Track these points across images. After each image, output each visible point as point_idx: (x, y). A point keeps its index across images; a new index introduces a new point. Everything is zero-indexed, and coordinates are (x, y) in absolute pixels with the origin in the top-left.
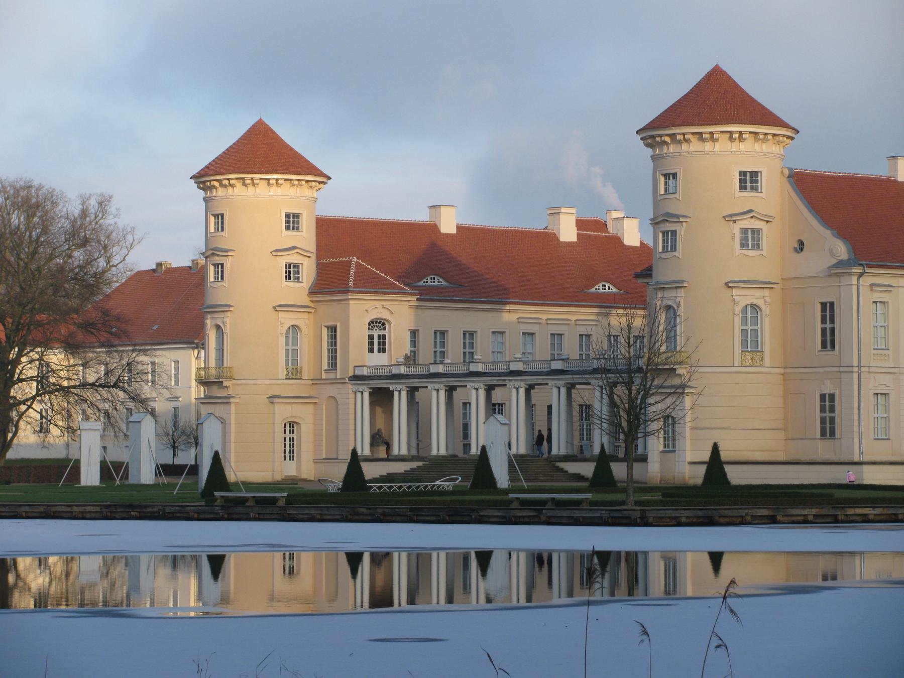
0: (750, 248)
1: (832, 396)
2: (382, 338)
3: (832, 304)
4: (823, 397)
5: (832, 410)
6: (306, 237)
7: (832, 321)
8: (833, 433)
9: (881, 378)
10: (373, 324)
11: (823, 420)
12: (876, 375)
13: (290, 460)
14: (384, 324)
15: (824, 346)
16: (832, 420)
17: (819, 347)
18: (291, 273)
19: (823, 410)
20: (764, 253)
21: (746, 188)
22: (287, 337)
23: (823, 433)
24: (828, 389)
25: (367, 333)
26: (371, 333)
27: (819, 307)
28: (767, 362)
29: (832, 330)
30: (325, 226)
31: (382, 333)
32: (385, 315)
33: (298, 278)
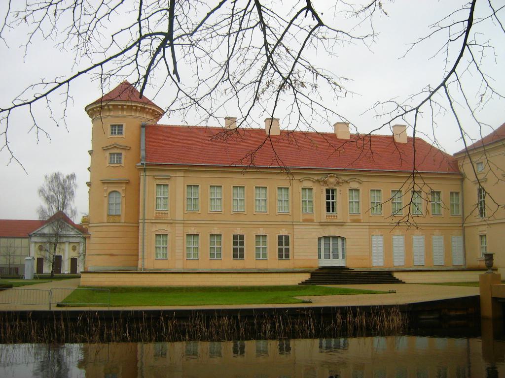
21: (115, 133)
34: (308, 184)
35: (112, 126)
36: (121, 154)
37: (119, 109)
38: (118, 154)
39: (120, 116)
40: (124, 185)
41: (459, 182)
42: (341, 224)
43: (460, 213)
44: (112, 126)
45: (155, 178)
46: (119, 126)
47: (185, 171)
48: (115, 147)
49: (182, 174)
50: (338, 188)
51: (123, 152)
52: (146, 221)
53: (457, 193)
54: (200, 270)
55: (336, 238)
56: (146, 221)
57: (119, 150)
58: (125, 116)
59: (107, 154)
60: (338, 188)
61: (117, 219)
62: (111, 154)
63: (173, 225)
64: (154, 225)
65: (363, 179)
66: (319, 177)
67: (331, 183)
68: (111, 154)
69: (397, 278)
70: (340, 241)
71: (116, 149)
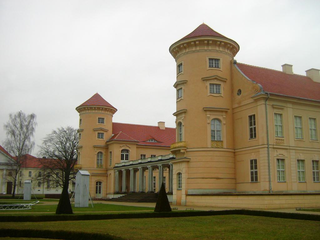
0: (215, 93)
1: (256, 161)
3: (254, 115)
4: (252, 161)
5: (256, 168)
8: (256, 179)
10: (122, 151)
11: (252, 173)
12: (278, 150)
13: (99, 193)
14: (127, 151)
15: (251, 136)
16: (256, 172)
20: (222, 95)
23: (252, 180)
25: (121, 153)
26: (122, 153)
27: (248, 119)
28: (225, 146)
31: (127, 154)
32: (127, 148)
33: (103, 138)
35: (210, 59)
36: (219, 85)
37: (192, 46)
38: (216, 85)
39: (217, 51)
40: (224, 114)
44: (210, 59)
45: (273, 107)
46: (215, 60)
47: (293, 103)
48: (216, 79)
49: (290, 105)
51: (222, 84)
52: (270, 146)
54: (309, 192)
56: (267, 146)
57: (219, 81)
58: (221, 52)
59: (208, 84)
61: (219, 144)
62: (210, 84)
63: (288, 150)
64: (275, 150)
68: (210, 84)
71: (216, 80)
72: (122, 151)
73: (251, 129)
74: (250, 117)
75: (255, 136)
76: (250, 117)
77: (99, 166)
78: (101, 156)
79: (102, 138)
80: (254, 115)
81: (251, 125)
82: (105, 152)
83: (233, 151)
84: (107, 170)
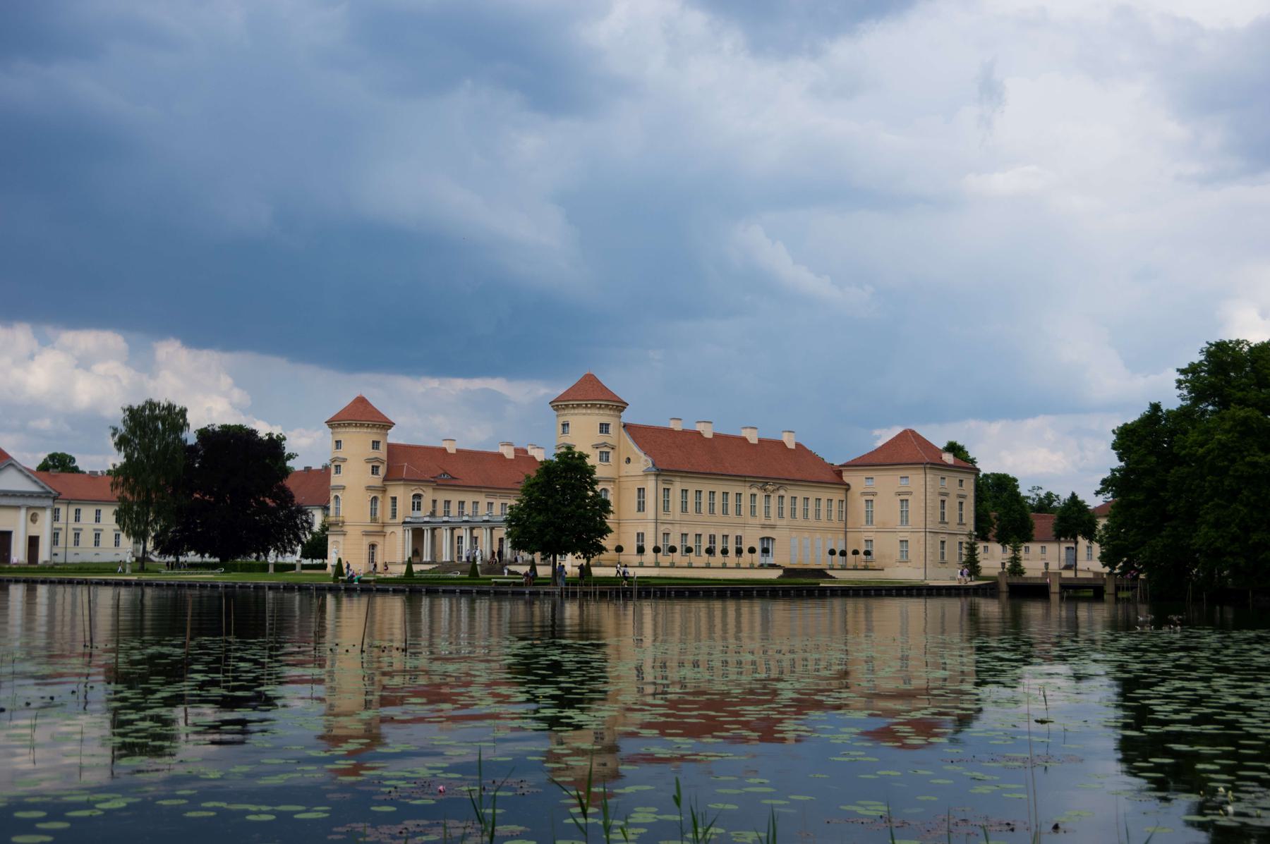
1: (643, 534)
2: (419, 504)
3: (644, 489)
4: (638, 534)
5: (643, 541)
6: (382, 453)
7: (644, 497)
9: (666, 526)
15: (639, 510)
17: (636, 509)
18: (375, 470)
19: (638, 541)
22: (372, 503)
24: (640, 531)
25: (411, 501)
29: (644, 502)
30: (392, 448)
31: (419, 501)
32: (421, 492)
34: (754, 491)
36: (608, 452)
40: (612, 483)
41: (844, 492)
42: (773, 527)
43: (844, 519)
47: (682, 477)
49: (678, 479)
50: (772, 495)
51: (611, 451)
53: (842, 501)
55: (768, 538)
60: (772, 495)
62: (600, 452)
65: (788, 487)
66: (761, 485)
67: (769, 491)
69: (830, 574)
70: (771, 542)
72: (414, 495)
73: (639, 503)
74: (639, 490)
75: (644, 510)
76: (639, 489)
77: (374, 519)
78: (376, 502)
79: (377, 474)
80: (644, 489)
81: (639, 497)
82: (382, 497)
83: (617, 521)
84: (384, 526)
